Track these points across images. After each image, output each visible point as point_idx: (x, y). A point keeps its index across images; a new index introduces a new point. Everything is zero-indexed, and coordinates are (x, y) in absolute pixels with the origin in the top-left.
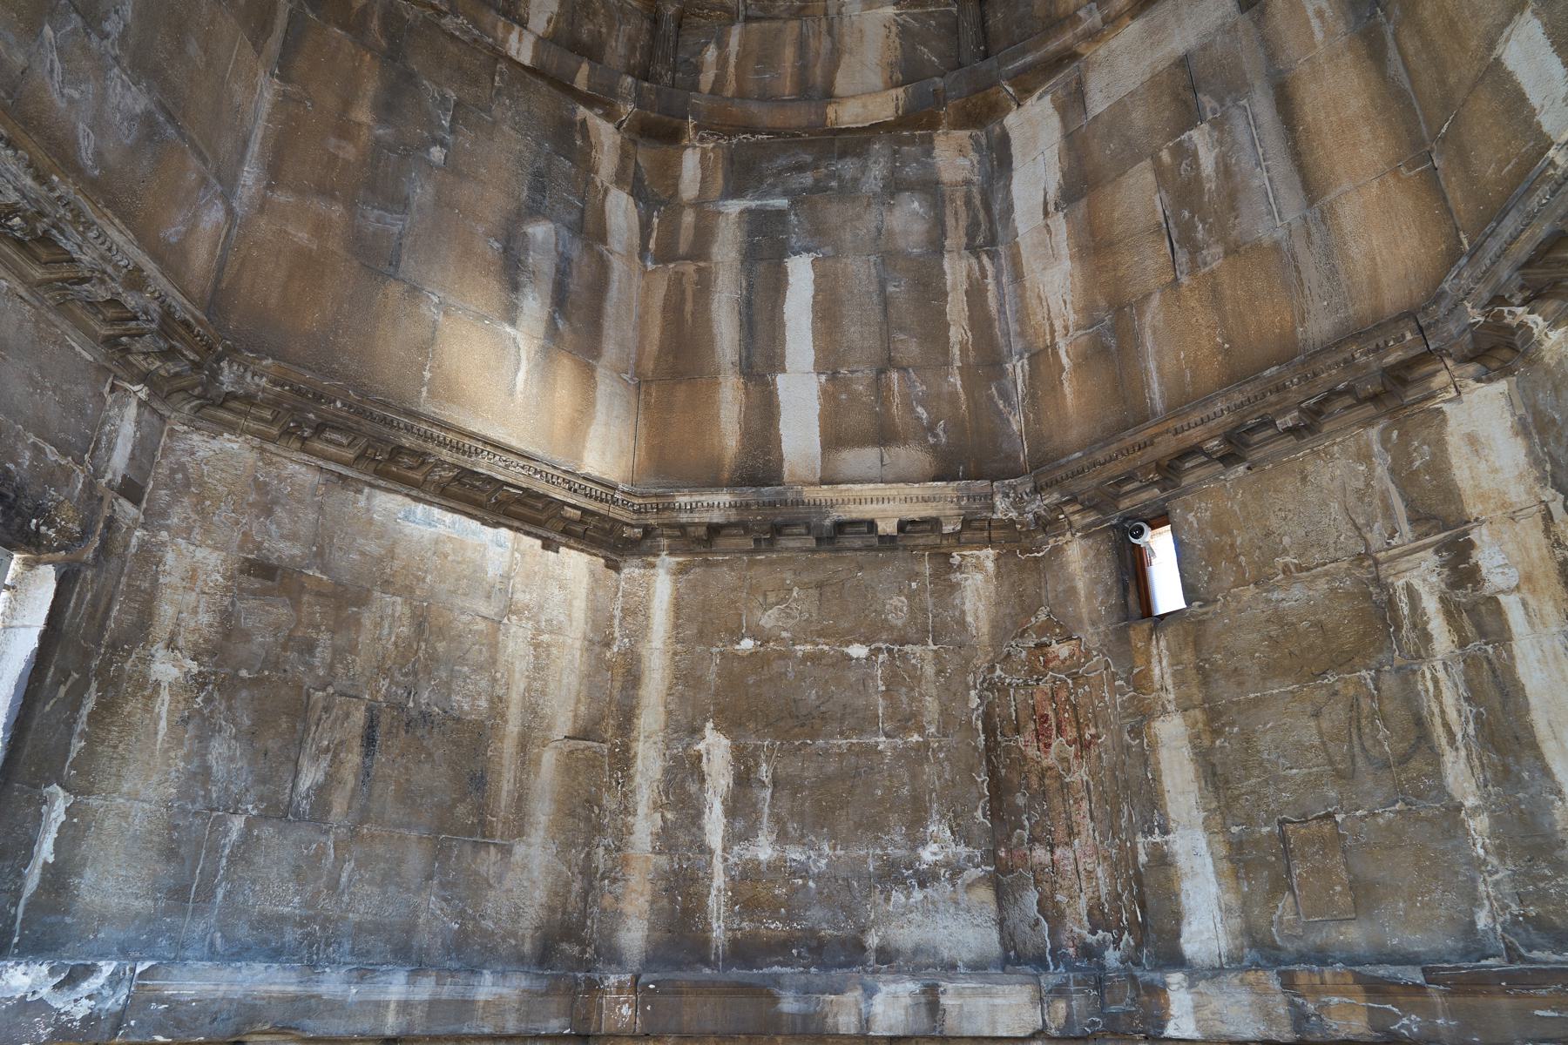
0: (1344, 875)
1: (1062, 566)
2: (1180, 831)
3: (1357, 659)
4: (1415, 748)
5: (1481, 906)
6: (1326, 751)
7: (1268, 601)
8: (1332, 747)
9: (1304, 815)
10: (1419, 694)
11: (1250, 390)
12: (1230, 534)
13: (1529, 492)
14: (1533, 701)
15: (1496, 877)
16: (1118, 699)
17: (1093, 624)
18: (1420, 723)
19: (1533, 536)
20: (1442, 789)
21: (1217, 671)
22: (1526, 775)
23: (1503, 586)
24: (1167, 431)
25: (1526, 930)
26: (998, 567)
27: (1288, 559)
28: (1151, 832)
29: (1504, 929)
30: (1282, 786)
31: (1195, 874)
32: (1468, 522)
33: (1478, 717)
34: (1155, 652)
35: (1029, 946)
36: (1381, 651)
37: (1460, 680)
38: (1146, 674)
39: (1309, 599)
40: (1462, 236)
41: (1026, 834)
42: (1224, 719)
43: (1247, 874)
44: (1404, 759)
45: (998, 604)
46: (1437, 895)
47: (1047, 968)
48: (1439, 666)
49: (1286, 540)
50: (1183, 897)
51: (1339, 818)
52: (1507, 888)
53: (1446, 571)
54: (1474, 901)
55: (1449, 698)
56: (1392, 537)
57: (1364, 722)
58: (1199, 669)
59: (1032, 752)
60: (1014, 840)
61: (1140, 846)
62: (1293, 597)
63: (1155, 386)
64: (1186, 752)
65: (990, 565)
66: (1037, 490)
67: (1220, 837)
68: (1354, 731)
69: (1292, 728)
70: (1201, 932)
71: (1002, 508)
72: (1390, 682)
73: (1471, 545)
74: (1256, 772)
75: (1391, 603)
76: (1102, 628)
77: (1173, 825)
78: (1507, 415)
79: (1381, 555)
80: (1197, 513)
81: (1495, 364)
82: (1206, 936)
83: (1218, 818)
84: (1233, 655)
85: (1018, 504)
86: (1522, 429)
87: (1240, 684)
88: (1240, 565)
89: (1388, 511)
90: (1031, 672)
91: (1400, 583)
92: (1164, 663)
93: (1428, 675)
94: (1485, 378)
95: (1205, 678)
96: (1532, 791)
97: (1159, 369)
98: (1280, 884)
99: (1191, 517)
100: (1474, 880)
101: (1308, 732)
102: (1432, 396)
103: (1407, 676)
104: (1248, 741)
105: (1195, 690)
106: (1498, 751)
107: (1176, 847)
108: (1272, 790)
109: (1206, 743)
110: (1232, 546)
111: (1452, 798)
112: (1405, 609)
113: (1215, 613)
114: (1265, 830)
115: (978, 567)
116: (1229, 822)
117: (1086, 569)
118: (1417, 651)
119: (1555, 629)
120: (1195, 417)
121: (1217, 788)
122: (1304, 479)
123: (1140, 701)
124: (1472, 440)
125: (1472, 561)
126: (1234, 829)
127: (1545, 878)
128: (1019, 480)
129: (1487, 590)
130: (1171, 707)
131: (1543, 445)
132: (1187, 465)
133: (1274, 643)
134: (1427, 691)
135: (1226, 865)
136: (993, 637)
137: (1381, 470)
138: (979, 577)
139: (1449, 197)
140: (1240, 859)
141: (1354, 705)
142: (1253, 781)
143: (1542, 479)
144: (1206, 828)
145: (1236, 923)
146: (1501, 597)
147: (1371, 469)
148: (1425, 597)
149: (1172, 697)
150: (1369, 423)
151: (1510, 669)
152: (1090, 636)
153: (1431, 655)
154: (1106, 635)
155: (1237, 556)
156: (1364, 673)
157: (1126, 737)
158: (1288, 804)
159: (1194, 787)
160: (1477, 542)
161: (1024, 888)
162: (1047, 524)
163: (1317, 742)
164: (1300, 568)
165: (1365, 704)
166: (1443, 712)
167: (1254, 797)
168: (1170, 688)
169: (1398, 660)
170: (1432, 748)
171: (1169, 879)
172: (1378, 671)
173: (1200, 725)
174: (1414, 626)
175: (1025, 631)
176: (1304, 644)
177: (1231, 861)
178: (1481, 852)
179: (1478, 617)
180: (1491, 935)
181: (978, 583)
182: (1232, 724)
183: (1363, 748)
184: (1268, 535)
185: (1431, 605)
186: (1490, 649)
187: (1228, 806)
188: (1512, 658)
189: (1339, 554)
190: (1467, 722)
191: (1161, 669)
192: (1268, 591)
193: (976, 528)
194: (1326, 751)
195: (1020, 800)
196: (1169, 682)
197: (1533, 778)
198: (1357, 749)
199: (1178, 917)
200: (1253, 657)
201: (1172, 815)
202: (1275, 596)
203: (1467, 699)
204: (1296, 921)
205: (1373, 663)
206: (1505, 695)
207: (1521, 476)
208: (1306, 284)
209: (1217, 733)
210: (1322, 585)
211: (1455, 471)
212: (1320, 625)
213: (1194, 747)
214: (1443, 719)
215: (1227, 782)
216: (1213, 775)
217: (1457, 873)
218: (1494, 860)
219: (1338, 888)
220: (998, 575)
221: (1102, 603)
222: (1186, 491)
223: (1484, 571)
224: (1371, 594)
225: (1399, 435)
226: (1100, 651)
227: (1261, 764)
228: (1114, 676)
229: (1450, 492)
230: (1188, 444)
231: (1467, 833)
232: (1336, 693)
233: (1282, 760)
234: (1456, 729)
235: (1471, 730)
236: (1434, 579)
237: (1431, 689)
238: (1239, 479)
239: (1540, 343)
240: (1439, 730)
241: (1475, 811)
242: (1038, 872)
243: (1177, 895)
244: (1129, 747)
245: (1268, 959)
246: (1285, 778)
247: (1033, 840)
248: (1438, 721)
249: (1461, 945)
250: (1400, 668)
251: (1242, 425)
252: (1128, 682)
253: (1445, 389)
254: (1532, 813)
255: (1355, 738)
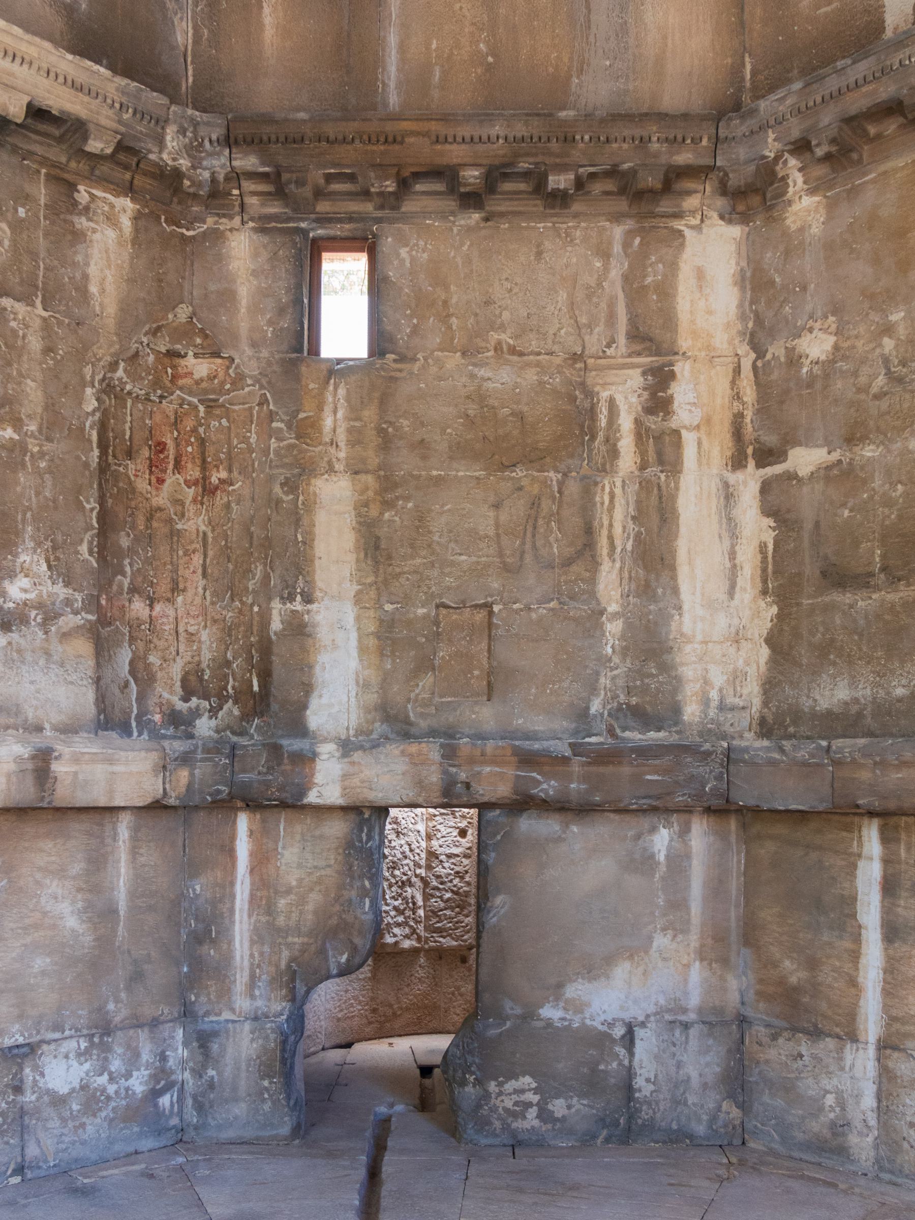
0: (485, 661)
1: (220, 259)
2: (326, 602)
3: (548, 460)
4: (580, 554)
5: (598, 695)
6: (499, 543)
7: (472, 376)
8: (505, 540)
9: (464, 602)
10: (595, 504)
11: (536, 128)
12: (446, 288)
13: (730, 342)
14: (683, 530)
15: (615, 672)
16: (273, 443)
17: (254, 345)
18: (589, 531)
19: (723, 386)
20: (592, 594)
21: (401, 438)
22: (660, 591)
23: (687, 423)
24: (426, 134)
25: (626, 716)
26: (136, 230)
27: (503, 337)
28: (291, 598)
29: (610, 715)
30: (447, 570)
31: (335, 647)
32: (676, 353)
33: (638, 535)
34: (330, 399)
35: (117, 710)
36: (572, 456)
37: (632, 499)
38: (315, 423)
39: (516, 385)
40: (747, 59)
41: (126, 583)
42: (399, 492)
43: (393, 652)
44: (568, 563)
45: (131, 281)
46: (565, 684)
47: (129, 734)
48: (619, 483)
49: (506, 315)
50: (317, 669)
51: (496, 608)
52: (621, 682)
53: (646, 395)
54: (593, 690)
55: (618, 514)
56: (609, 346)
57: (540, 522)
58: (381, 432)
59: (142, 485)
60: (115, 588)
61: (275, 613)
62: (500, 378)
63: (392, 69)
64: (349, 519)
65: (126, 223)
66: (229, 141)
67: (372, 613)
68: (530, 529)
69: (469, 512)
70: (331, 705)
71: (171, 149)
72: (573, 488)
73: (672, 376)
74: (424, 553)
75: (592, 413)
76: (265, 353)
77: (318, 594)
78: (733, 262)
79: (591, 361)
80: (406, 251)
81: (741, 208)
82: (336, 709)
83: (373, 594)
84: (422, 424)
85: (194, 150)
86: (741, 281)
87: (424, 458)
88: (450, 327)
89: (611, 318)
90: (157, 383)
91: (605, 395)
92: (340, 415)
93: (607, 489)
94: (726, 218)
95: (386, 442)
96: (661, 605)
97: (402, 48)
98: (424, 665)
99: (404, 252)
100: (597, 674)
101: (485, 521)
102: (678, 216)
103: (588, 488)
104: (421, 519)
105: (371, 453)
106: (645, 567)
107: (319, 618)
108: (435, 573)
109: (374, 512)
110: (445, 302)
111: (599, 603)
112: (603, 421)
113: (411, 373)
114: (421, 611)
115: (112, 219)
116: (384, 599)
117: (255, 274)
118: (604, 465)
119: (715, 471)
120: (465, 131)
121: (377, 563)
122: (539, 254)
123: (300, 452)
124: (700, 274)
125: (670, 392)
126: (388, 607)
127: (652, 676)
128: (205, 117)
129: (674, 424)
130: (339, 467)
131: (752, 303)
132: (418, 187)
133: (470, 422)
134: (602, 504)
135: (372, 642)
136: (120, 323)
137: (615, 273)
138: (111, 234)
139: (747, 10)
140: (387, 638)
141: (535, 504)
142: (418, 561)
143: (742, 334)
144: (358, 599)
145: (373, 698)
146: (684, 433)
147: (606, 269)
148: (623, 414)
149: (342, 455)
150: (616, 218)
151: (673, 498)
152: (248, 360)
153: (613, 471)
154: (269, 364)
155: (449, 316)
156: (552, 474)
157: (277, 490)
158: (449, 588)
159: (352, 557)
160: (678, 375)
161: (119, 644)
162: (216, 196)
163: (491, 532)
164: (513, 351)
165: (546, 504)
166: (611, 525)
167: (416, 577)
168: (342, 445)
169: (585, 469)
170: (593, 557)
171: (304, 650)
172: (565, 475)
173: (370, 493)
174: (607, 440)
175: (159, 329)
176: (501, 432)
177: (379, 638)
178: (610, 650)
179: (661, 449)
180: (599, 718)
181: (108, 240)
182: (407, 499)
183: (534, 547)
184: (487, 303)
185: (626, 423)
186: (663, 476)
187: (386, 582)
188: (677, 489)
189: (556, 348)
190: (628, 538)
191: (334, 420)
192: (475, 365)
193: (128, 164)
194: (499, 543)
195: (125, 542)
196: (342, 437)
197: (664, 594)
198: (528, 546)
199: (308, 688)
200: (443, 432)
201: (320, 584)
202: (482, 372)
203: (634, 518)
204: (430, 699)
205: (562, 467)
206: (664, 520)
207: (728, 325)
208: (594, 29)
209: (388, 505)
210: (531, 376)
211: (679, 299)
212: (520, 416)
213: (359, 515)
214: (610, 531)
215: (390, 557)
216: (374, 547)
217: (586, 667)
218: (616, 660)
219: (476, 673)
220: (135, 241)
221: (270, 323)
222: (406, 218)
223: (676, 404)
224: (576, 398)
225: (641, 244)
226: (258, 381)
227: (429, 546)
228: (271, 416)
229: (670, 321)
230: (445, 161)
231: (603, 635)
232: (520, 489)
233: (452, 545)
234: (618, 543)
235: (629, 547)
236: (634, 399)
237: (607, 502)
238: (469, 229)
239: (790, 203)
240: (603, 542)
241: (616, 616)
242: (134, 625)
243: (311, 667)
244: (279, 502)
245: (398, 733)
246: (453, 564)
247: (134, 590)
248: (605, 532)
249: (574, 725)
250: (585, 477)
251: (511, 164)
252: (289, 427)
253: (693, 213)
254: (656, 623)
255: (529, 535)
